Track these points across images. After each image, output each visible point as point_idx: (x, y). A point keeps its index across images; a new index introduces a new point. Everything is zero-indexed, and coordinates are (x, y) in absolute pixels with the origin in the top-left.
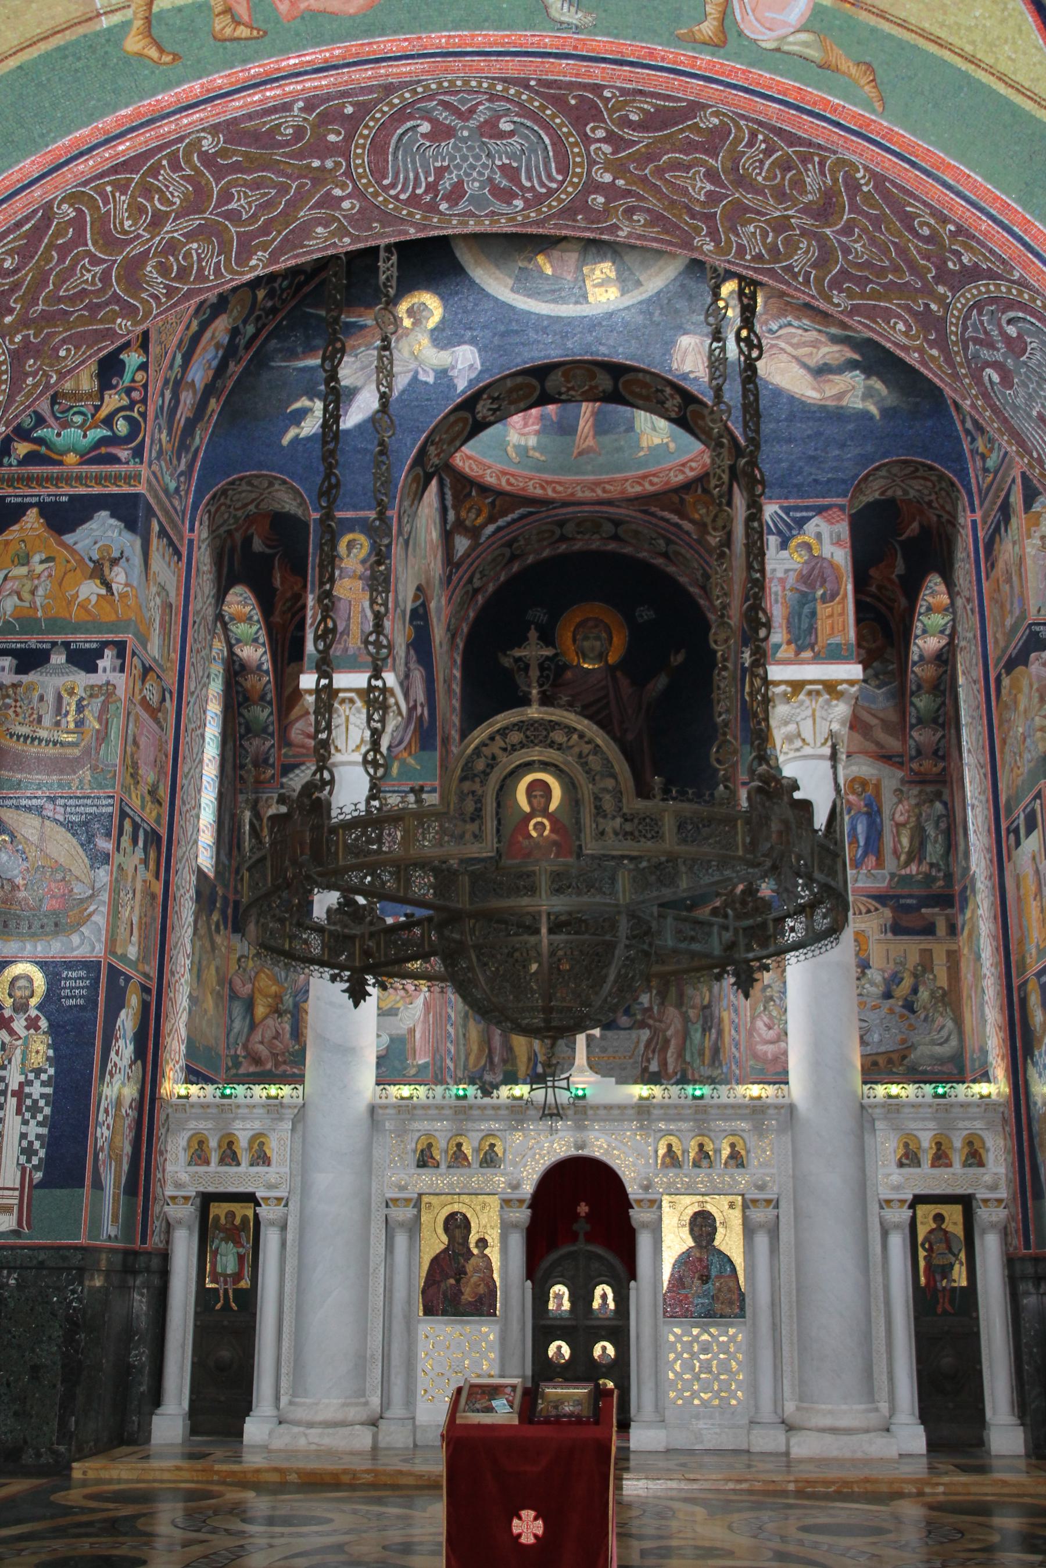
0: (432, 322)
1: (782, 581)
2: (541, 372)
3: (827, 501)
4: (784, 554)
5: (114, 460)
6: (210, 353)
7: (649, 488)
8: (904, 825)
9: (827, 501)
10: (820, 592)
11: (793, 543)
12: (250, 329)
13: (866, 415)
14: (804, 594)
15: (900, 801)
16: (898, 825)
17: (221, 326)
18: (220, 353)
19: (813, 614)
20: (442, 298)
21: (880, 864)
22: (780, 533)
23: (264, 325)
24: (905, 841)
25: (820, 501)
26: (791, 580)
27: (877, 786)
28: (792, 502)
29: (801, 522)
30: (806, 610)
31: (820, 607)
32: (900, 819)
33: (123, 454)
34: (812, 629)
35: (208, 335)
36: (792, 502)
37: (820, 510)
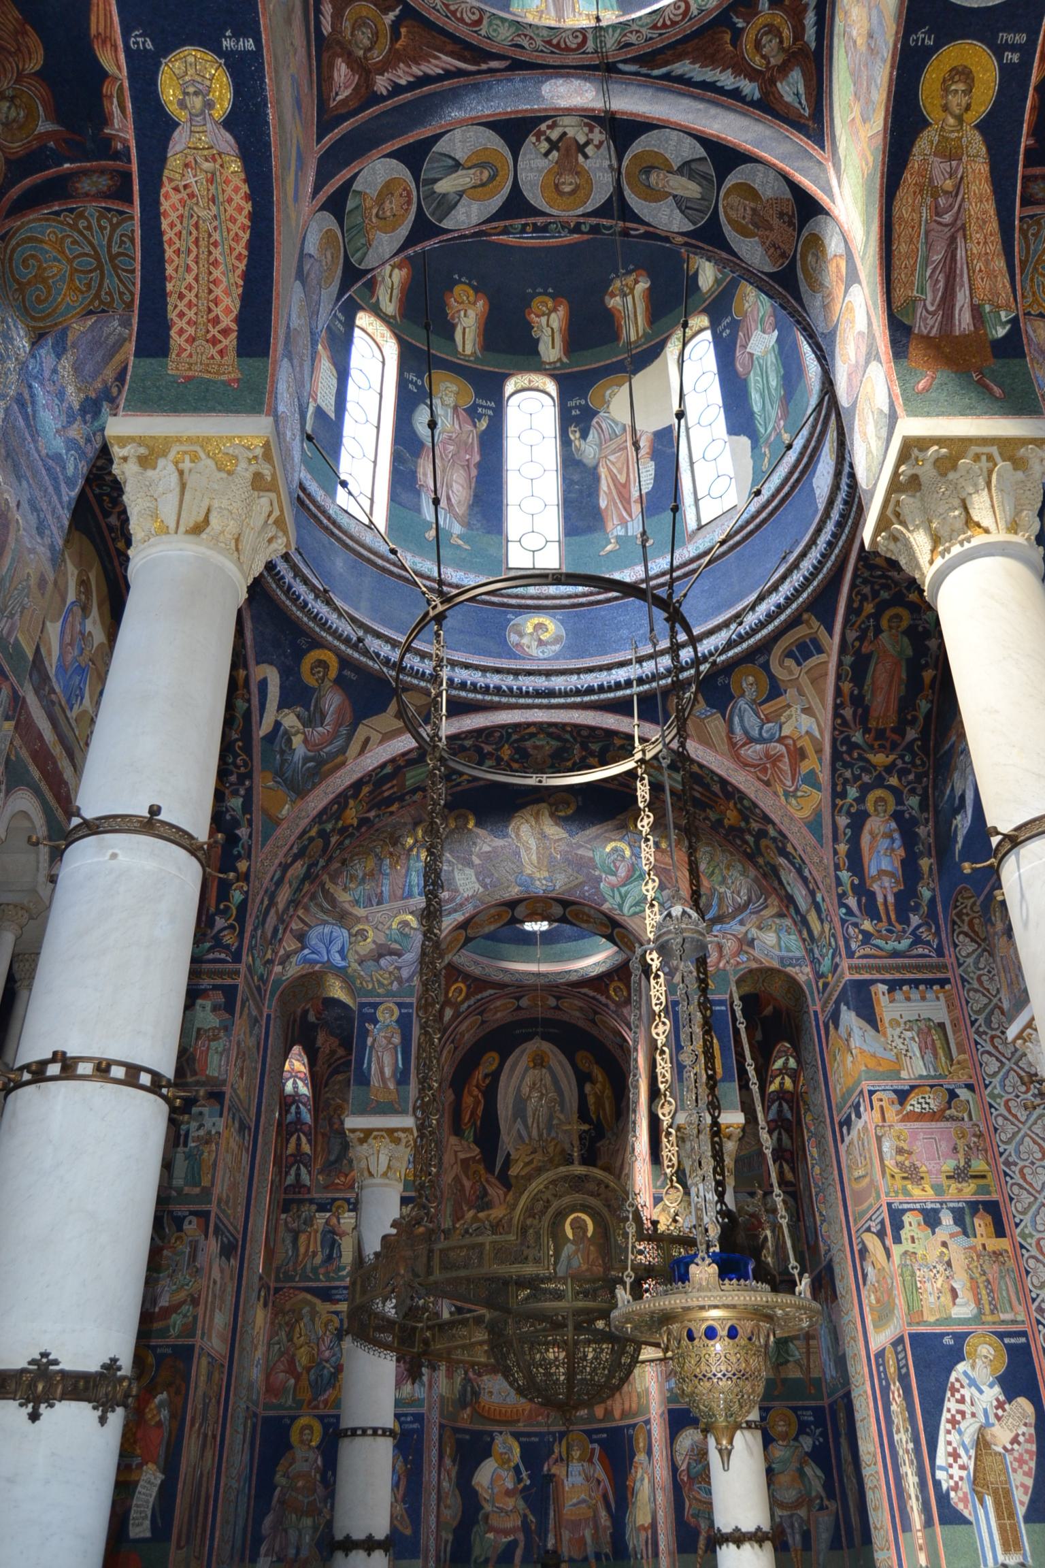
5: (837, 966)
6: (884, 844)
12: (913, 801)
17: (877, 825)
18: (896, 835)
23: (926, 789)
33: (837, 959)
35: (865, 839)
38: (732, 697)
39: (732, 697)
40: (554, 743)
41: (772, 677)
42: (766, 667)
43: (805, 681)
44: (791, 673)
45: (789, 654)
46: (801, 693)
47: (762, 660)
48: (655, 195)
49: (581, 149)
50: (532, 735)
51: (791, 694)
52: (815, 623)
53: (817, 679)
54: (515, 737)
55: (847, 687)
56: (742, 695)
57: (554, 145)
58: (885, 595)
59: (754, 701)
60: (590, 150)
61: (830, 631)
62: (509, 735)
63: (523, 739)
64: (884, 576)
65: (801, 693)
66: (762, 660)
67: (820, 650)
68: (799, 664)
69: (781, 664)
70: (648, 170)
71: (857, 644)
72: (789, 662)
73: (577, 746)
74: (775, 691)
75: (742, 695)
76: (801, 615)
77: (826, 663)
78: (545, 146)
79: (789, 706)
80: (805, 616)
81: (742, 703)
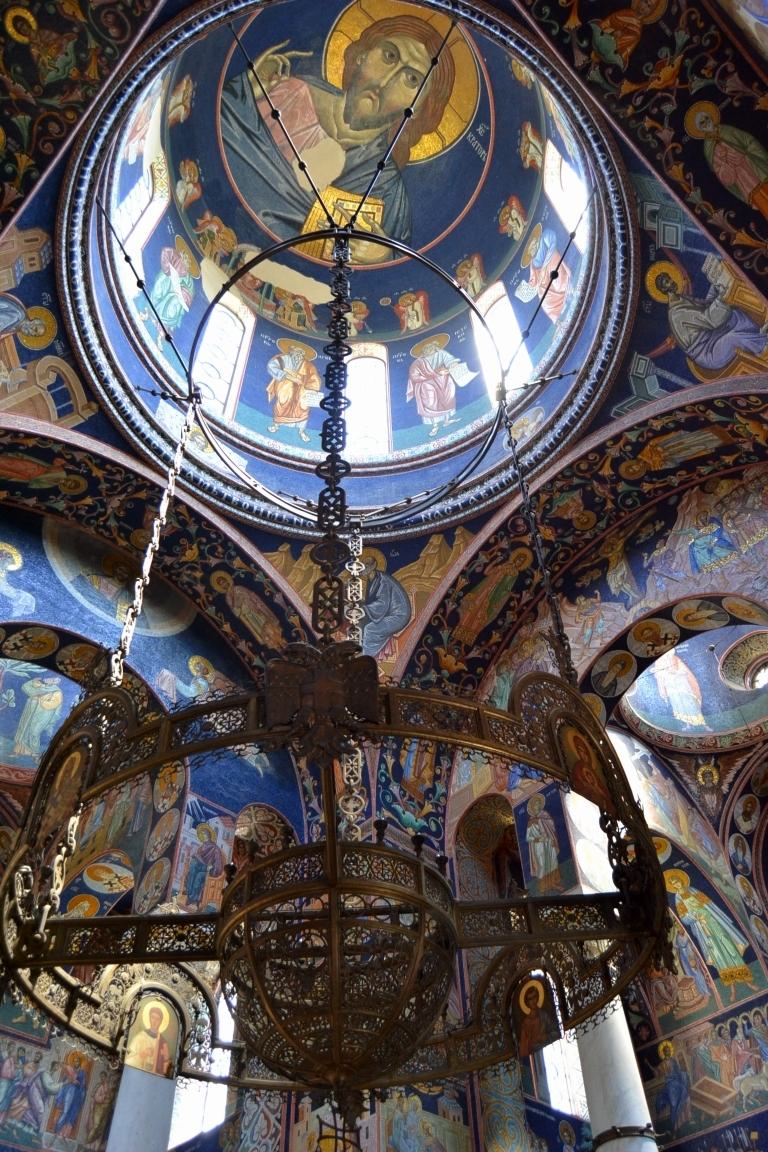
0: (12, 568)
1: (189, 849)
2: (67, 638)
3: (226, 811)
4: (194, 831)
7: (13, 778)
8: (100, 1104)
9: (226, 811)
10: (210, 868)
11: (200, 827)
13: (255, 771)
14: (200, 864)
15: (103, 1083)
16: (96, 1103)
19: (203, 880)
20: (24, 557)
21: (73, 1134)
22: (194, 816)
24: (97, 1119)
25: (221, 808)
26: (195, 850)
27: (90, 1065)
28: (205, 800)
29: (208, 816)
30: (199, 876)
31: (208, 878)
32: (99, 1098)
34: (200, 891)
36: (205, 800)
37: (221, 814)
38: (28, 305)
39: (28, 305)
40: (50, 77)
41: (39, 355)
42: (50, 350)
43: (32, 391)
44: (42, 377)
45: (60, 380)
46: (21, 385)
47: (58, 348)
48: (613, 663)
49: (653, 646)
50: (82, 66)
51: (22, 374)
52: (88, 414)
53: (31, 407)
54: (93, 44)
55: (31, 443)
56: (27, 318)
57: (666, 638)
58: (104, 486)
59: (19, 329)
60: (650, 648)
61: (79, 429)
62: (103, 43)
63: (81, 46)
64: (124, 491)
65: (21, 385)
66: (58, 348)
67: (62, 413)
68: (50, 388)
69: (52, 368)
70: (624, 666)
71: (69, 457)
72: (52, 379)
73: (30, 97)
74: (27, 356)
75: (27, 318)
76: (97, 401)
77: (49, 419)
78: (670, 636)
79: (10, 369)
80: (94, 406)
81: (19, 315)
